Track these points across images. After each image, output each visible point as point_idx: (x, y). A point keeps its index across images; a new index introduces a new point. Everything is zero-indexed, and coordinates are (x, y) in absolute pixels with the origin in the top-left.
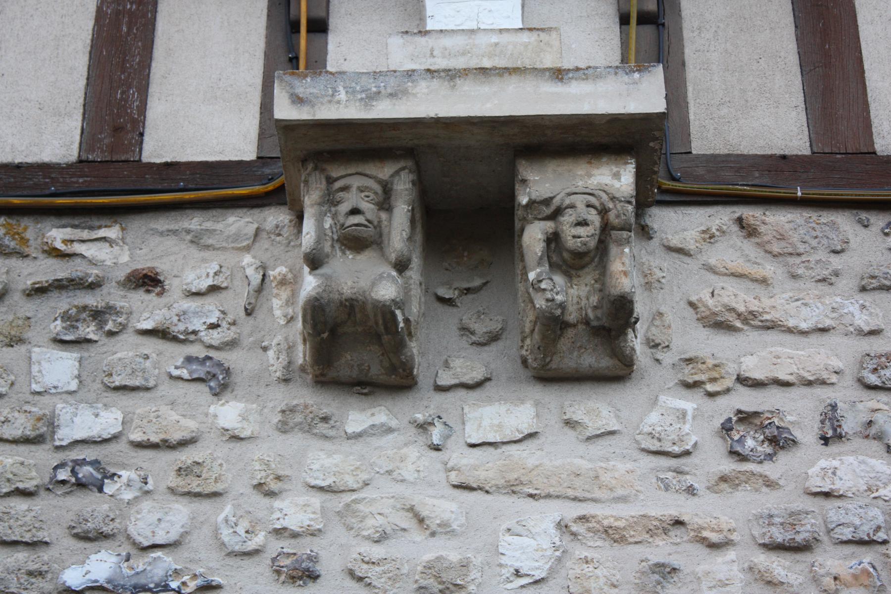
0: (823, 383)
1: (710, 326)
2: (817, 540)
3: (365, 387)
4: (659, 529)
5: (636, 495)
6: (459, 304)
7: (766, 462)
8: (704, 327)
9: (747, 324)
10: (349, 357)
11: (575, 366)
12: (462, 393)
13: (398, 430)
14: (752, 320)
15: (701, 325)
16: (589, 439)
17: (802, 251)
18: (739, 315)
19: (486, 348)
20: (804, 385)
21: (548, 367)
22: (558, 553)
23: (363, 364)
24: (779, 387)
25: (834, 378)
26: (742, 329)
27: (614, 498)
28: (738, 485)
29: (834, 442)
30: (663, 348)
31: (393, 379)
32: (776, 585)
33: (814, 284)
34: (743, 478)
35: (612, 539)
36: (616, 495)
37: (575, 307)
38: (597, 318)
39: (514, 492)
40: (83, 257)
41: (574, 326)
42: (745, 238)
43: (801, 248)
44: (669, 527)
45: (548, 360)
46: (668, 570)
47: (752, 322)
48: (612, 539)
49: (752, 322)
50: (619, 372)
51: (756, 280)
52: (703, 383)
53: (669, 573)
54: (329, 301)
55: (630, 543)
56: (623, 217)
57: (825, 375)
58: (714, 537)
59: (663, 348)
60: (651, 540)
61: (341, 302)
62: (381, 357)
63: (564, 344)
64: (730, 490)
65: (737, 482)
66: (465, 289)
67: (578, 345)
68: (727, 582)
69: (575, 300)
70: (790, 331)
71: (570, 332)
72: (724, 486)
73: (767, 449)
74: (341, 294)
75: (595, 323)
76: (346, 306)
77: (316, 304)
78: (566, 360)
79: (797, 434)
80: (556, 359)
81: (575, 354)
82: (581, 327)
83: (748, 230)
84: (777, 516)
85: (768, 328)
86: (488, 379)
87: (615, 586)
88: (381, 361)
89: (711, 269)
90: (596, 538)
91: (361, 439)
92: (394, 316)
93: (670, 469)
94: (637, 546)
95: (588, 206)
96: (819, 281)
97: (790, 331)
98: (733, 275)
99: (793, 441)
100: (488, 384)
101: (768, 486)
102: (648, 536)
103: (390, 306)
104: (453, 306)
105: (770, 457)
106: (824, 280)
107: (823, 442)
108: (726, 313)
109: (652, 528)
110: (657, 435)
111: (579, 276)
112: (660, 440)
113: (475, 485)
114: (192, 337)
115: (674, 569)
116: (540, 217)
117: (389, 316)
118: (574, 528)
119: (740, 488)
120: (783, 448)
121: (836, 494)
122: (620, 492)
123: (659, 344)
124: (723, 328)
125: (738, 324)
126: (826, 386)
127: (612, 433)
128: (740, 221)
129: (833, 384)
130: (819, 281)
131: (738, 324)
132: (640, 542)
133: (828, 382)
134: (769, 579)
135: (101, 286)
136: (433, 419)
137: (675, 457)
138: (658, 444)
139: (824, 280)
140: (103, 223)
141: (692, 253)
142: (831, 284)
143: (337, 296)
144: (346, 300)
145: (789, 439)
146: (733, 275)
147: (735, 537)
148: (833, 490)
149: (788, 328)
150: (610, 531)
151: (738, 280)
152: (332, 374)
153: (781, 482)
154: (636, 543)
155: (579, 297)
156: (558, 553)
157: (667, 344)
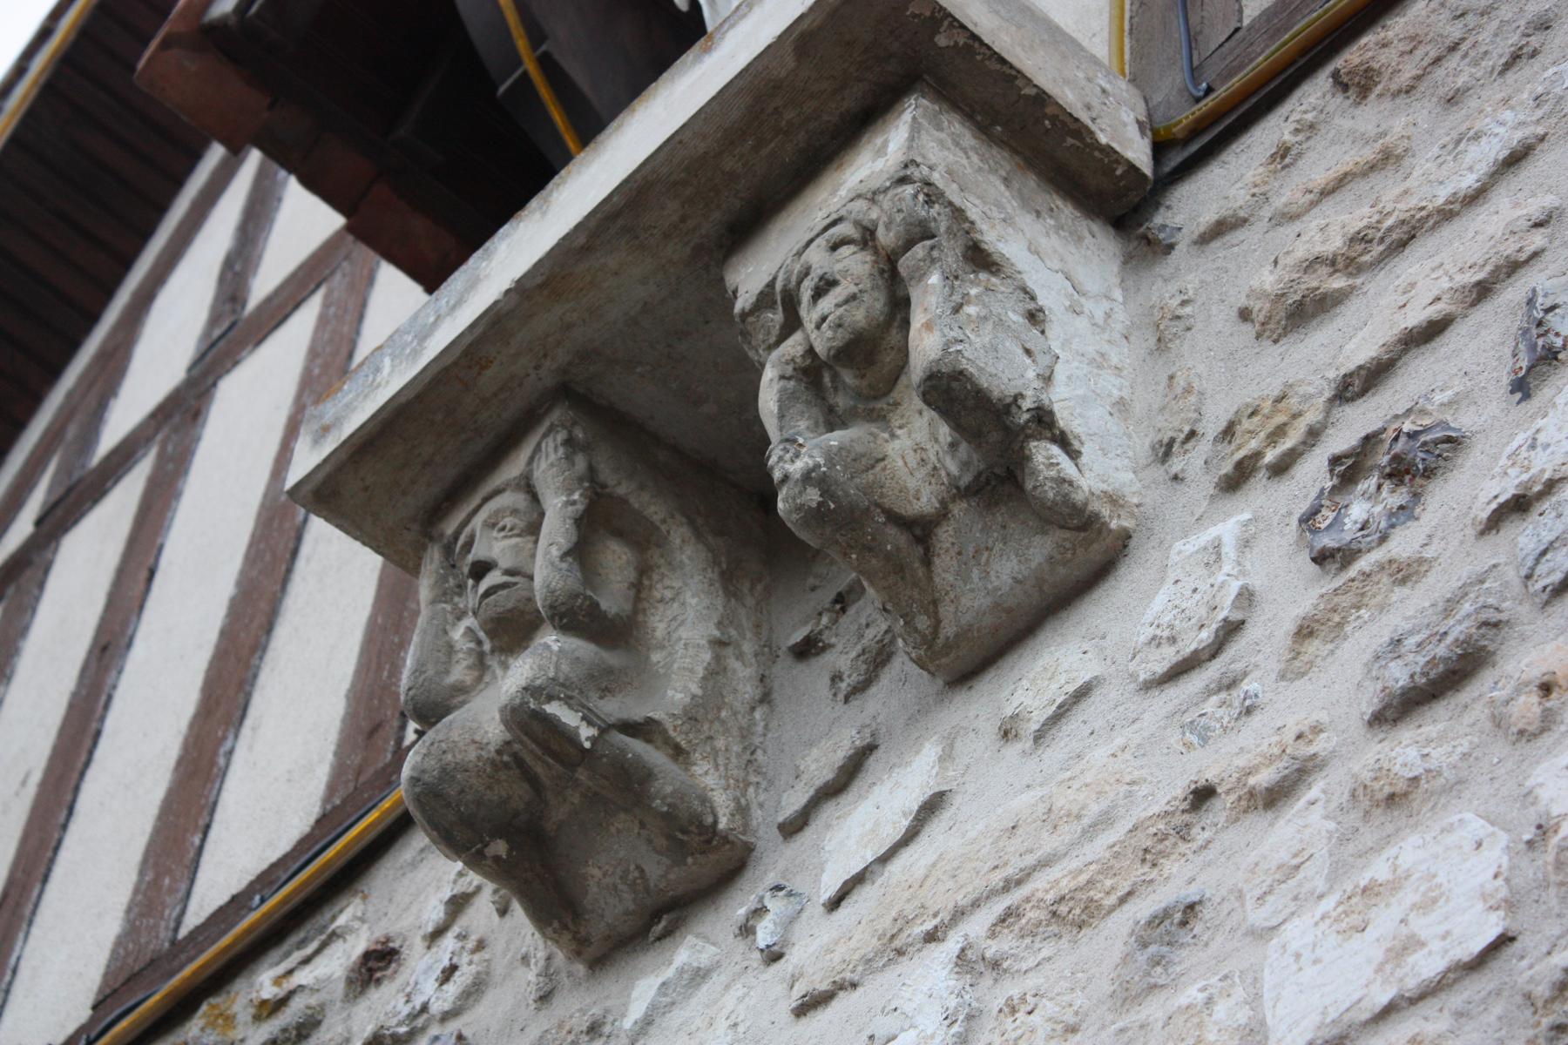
0: (1513, 267)
1: (1286, 332)
2: (1496, 625)
3: (662, 916)
4: (1165, 837)
5: (1129, 795)
6: (833, 640)
7: (1397, 530)
8: (1276, 342)
9: (1360, 269)
10: (597, 873)
11: (988, 601)
12: (829, 810)
13: (718, 965)
14: (1366, 251)
15: (1269, 342)
16: (1039, 737)
17: (1457, 35)
18: (1332, 262)
19: (873, 690)
20: (1473, 304)
21: (940, 641)
22: (956, 1028)
23: (626, 872)
24: (1423, 348)
25: (1538, 239)
26: (1353, 288)
27: (1084, 832)
28: (1340, 625)
29: (1543, 378)
30: (1184, 443)
31: (698, 868)
32: (1406, 795)
33: (1500, 81)
34: (1345, 600)
35: (1073, 923)
36: (1086, 821)
37: (922, 473)
38: (965, 465)
39: (900, 952)
40: (301, 987)
41: (943, 515)
42: (1357, 104)
43: (1455, 31)
44: (1186, 817)
45: (923, 622)
46: (1178, 916)
47: (1366, 258)
48: (1073, 923)
49: (1366, 258)
50: (1089, 554)
51: (1373, 167)
52: (1257, 455)
53: (1184, 923)
54: (443, 770)
55: (1112, 909)
56: (899, 218)
57: (1509, 248)
58: (1264, 778)
59: (1184, 443)
60: (1154, 874)
61: (493, 763)
62: (644, 833)
63: (945, 568)
64: (1330, 646)
65: (1337, 619)
66: (836, 601)
67: (971, 550)
68: (1295, 862)
69: (912, 460)
70: (1446, 215)
71: (945, 536)
72: (1313, 647)
73: (1394, 498)
74: (481, 746)
75: (966, 479)
76: (506, 765)
77: (417, 790)
78: (965, 601)
79: (1464, 421)
80: (946, 611)
81: (975, 573)
82: (958, 509)
83: (1359, 86)
84: (1411, 633)
85: (1403, 244)
86: (869, 749)
87: (1073, 1029)
88: (650, 841)
89: (1283, 215)
90: (1037, 945)
91: (653, 1030)
92: (551, 724)
93: (1209, 692)
94: (1126, 907)
95: (834, 247)
96: (1507, 67)
97: (1446, 215)
98: (1325, 193)
99: (1449, 440)
100: (872, 762)
101: (1403, 582)
102: (1146, 869)
103: (524, 703)
104: (824, 649)
105: (1404, 513)
106: (1516, 57)
107: (1518, 395)
108: (1306, 278)
109: (1149, 843)
110: (1166, 633)
111: (897, 404)
112: (1173, 640)
113: (824, 986)
114: (420, 1022)
115: (1191, 907)
116: (772, 340)
117: (537, 727)
118: (992, 949)
119: (1348, 629)
120: (1429, 473)
121: (1537, 488)
122: (1094, 809)
123: (1172, 441)
124: (1314, 316)
125: (1338, 283)
126: (1523, 271)
127: (1083, 693)
128: (1341, 84)
129: (1536, 255)
130: (1507, 67)
131: (1338, 283)
132: (1130, 894)
133: (1523, 257)
134: (1387, 790)
135: (319, 1023)
136: (761, 899)
137: (1213, 656)
138: (1173, 650)
139: (1516, 57)
140: (336, 909)
141: (1242, 214)
142: (1534, 54)
143: (472, 755)
144: (499, 752)
145: (1436, 442)
146: (1325, 193)
147: (1320, 746)
148: (1527, 485)
149: (1439, 211)
150: (1063, 909)
151: (1337, 197)
152: (597, 929)
153: (1429, 553)
154: (1123, 900)
155: (918, 448)
156: (956, 1028)
157: (1187, 429)
